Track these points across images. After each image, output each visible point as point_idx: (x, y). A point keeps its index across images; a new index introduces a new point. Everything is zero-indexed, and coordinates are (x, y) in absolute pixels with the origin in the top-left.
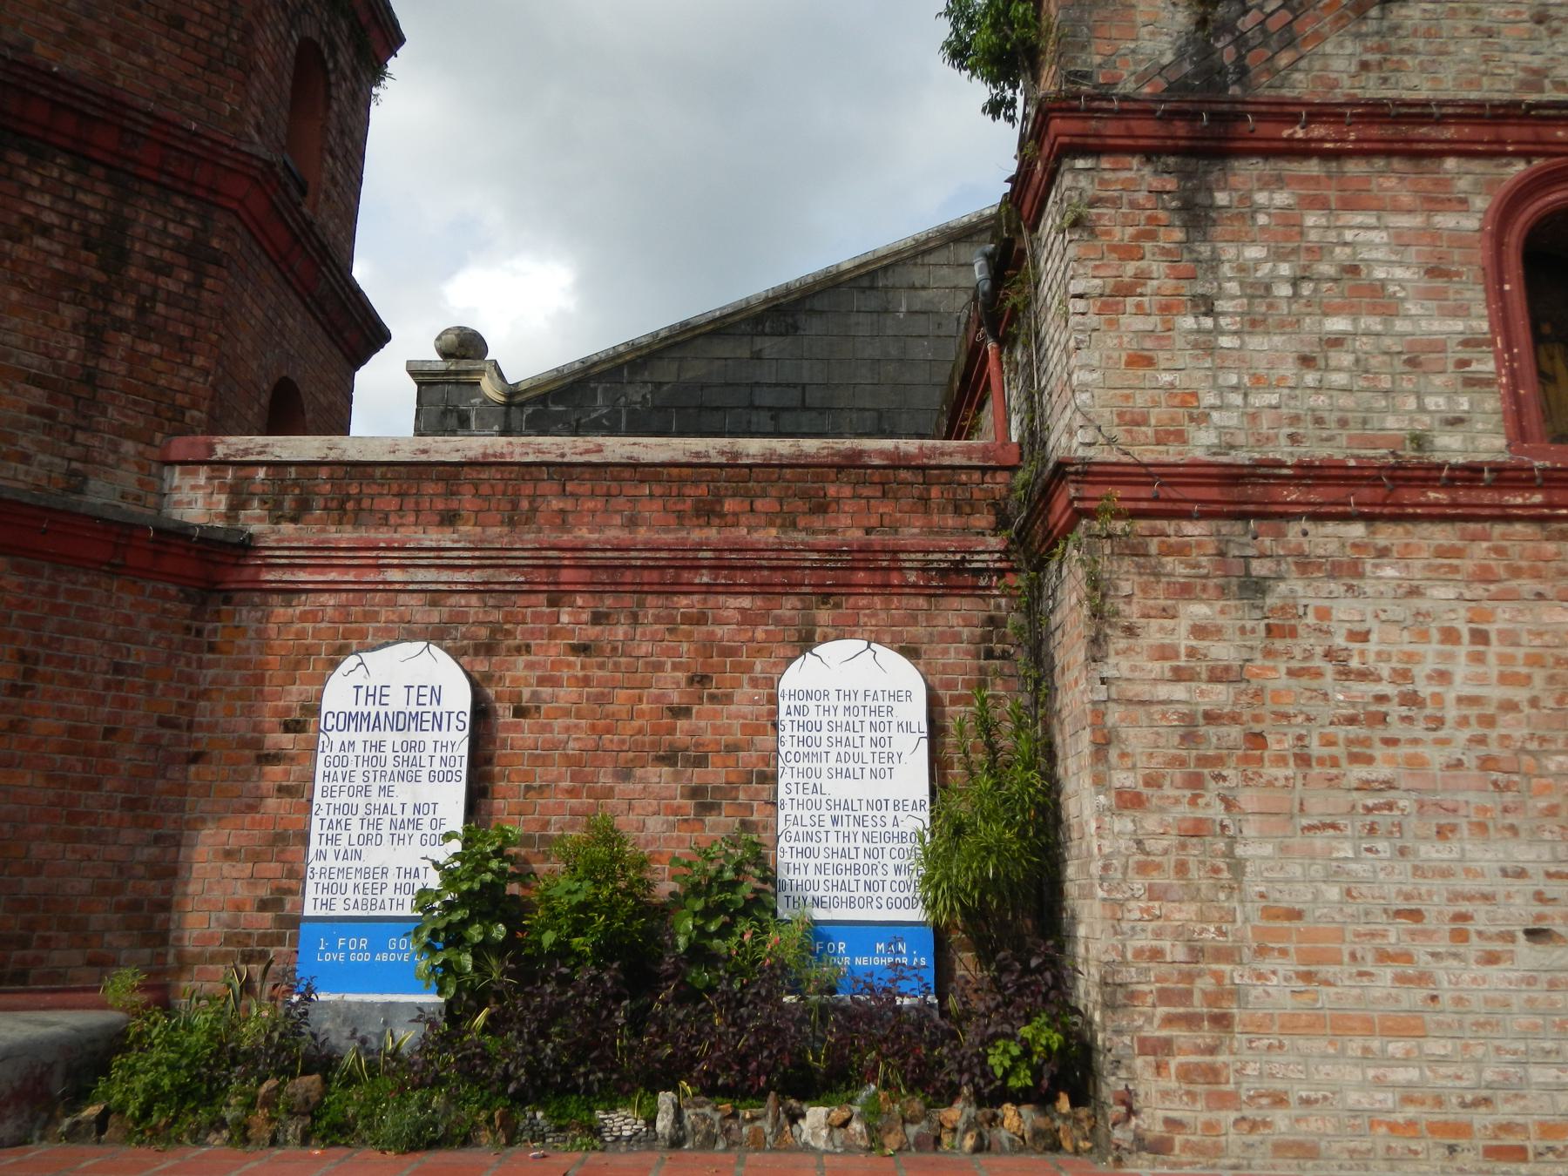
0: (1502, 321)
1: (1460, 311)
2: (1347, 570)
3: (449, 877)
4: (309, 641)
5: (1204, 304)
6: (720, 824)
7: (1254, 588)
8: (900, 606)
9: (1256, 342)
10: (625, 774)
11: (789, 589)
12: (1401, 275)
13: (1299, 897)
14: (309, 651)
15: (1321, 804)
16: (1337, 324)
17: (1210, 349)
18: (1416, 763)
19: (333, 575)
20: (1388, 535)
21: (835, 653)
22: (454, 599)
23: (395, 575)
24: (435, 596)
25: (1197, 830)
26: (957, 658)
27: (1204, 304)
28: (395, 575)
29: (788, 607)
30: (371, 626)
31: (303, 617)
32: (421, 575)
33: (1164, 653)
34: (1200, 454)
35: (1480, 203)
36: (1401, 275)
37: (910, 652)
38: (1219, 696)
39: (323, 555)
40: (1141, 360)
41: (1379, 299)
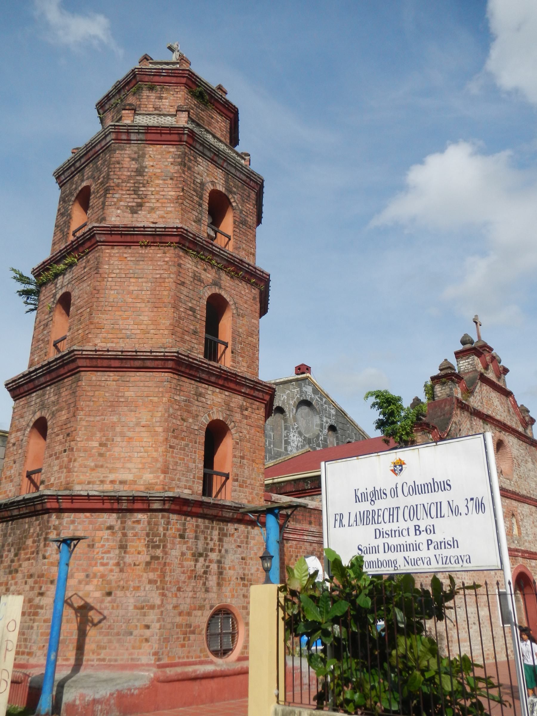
4: (291, 553)
14: (292, 556)
19: (295, 536)
22: (314, 545)
23: (305, 537)
24: (311, 543)
28: (305, 537)
30: (301, 550)
31: (291, 547)
32: (310, 538)
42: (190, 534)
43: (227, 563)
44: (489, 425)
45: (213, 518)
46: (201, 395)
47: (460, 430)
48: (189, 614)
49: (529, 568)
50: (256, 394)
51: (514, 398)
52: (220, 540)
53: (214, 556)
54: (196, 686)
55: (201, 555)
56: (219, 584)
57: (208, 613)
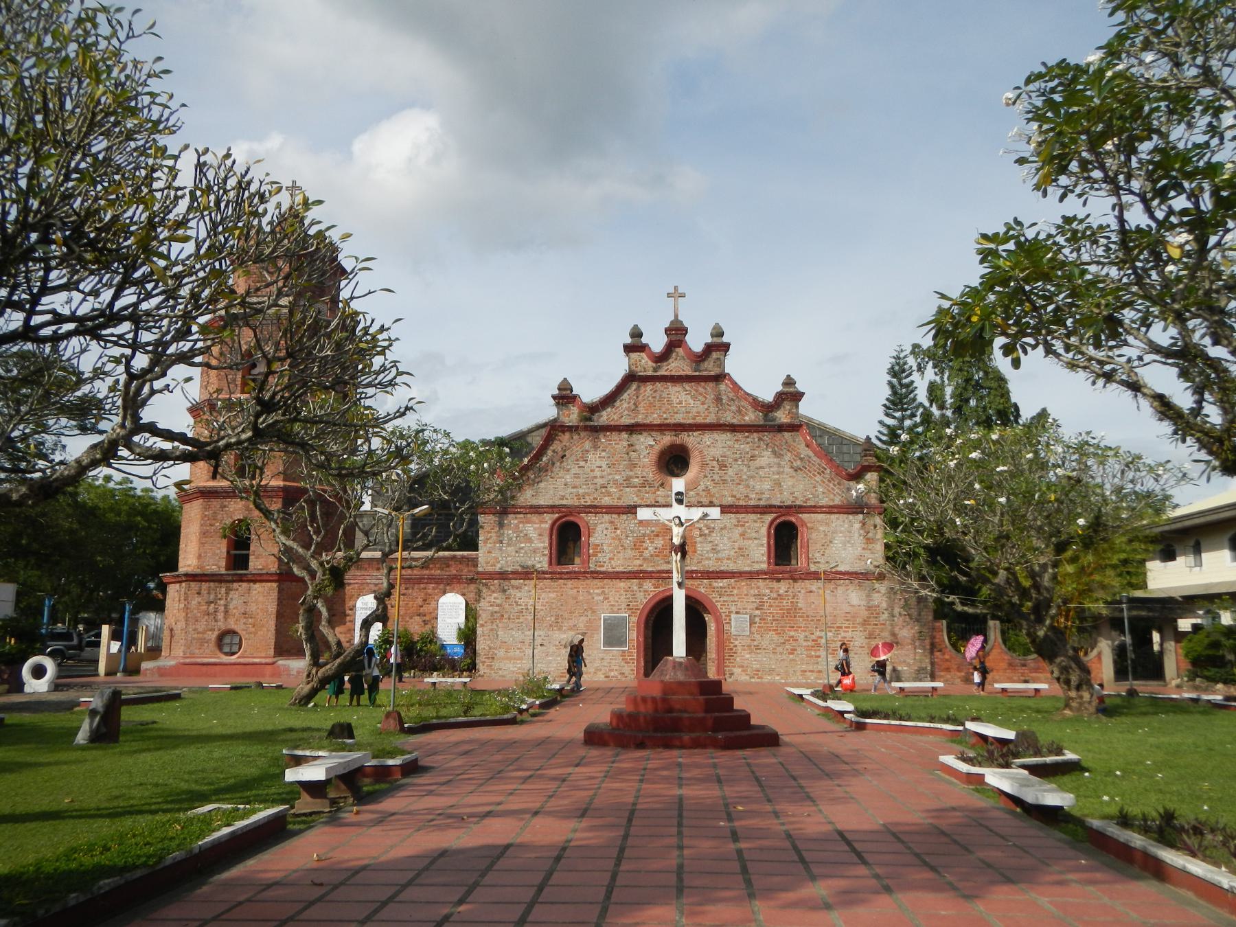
0: (551, 544)
1: (544, 542)
2: (519, 588)
3: (380, 637)
5: (501, 542)
6: (428, 627)
7: (504, 591)
8: (462, 586)
9: (509, 549)
10: (411, 618)
11: (442, 582)
12: (534, 535)
13: (507, 640)
15: (511, 626)
16: (523, 545)
17: (501, 550)
18: (526, 619)
20: (527, 582)
21: (448, 595)
25: (492, 630)
26: (472, 596)
27: (501, 542)
29: (442, 586)
33: (489, 602)
34: (497, 570)
35: (550, 522)
36: (534, 535)
37: (463, 595)
38: (497, 609)
39: (355, 577)
40: (489, 552)
41: (530, 540)
42: (204, 592)
43: (231, 606)
44: (645, 434)
45: (220, 581)
46: (225, 506)
47: (563, 456)
48: (204, 632)
49: (703, 590)
50: (270, 494)
51: (731, 379)
52: (227, 593)
53: (222, 602)
54: (204, 668)
55: (212, 602)
56: (225, 618)
57: (216, 633)
